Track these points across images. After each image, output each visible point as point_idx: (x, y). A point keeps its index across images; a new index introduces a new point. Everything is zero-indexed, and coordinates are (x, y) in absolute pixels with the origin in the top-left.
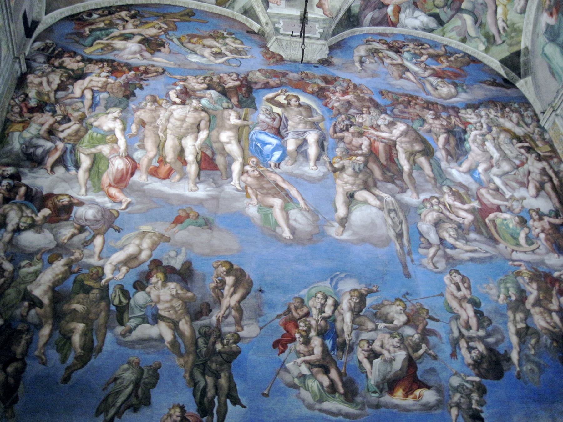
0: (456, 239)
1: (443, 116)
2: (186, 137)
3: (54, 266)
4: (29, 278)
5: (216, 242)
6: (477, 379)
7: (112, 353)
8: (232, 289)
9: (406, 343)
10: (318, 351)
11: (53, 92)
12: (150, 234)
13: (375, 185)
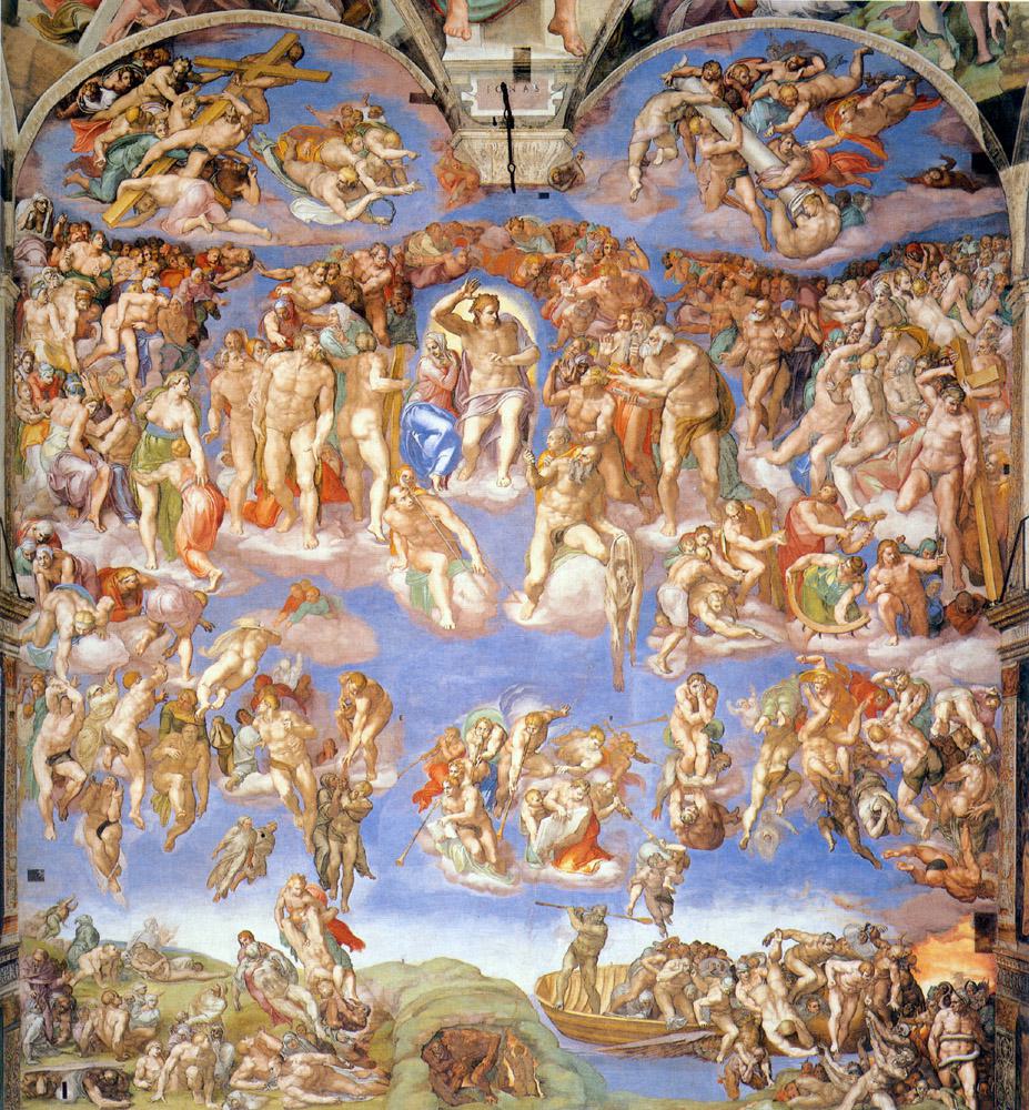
0: (718, 615)
1: (785, 314)
2: (297, 430)
3: (132, 691)
4: (105, 712)
5: (344, 641)
6: (681, 848)
7: (218, 812)
8: (364, 719)
9: (592, 795)
10: (470, 806)
11: (72, 343)
12: (253, 632)
13: (604, 513)
